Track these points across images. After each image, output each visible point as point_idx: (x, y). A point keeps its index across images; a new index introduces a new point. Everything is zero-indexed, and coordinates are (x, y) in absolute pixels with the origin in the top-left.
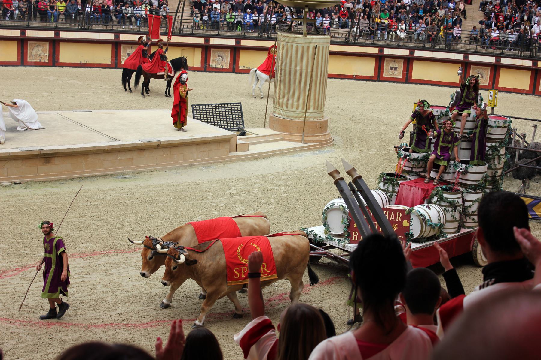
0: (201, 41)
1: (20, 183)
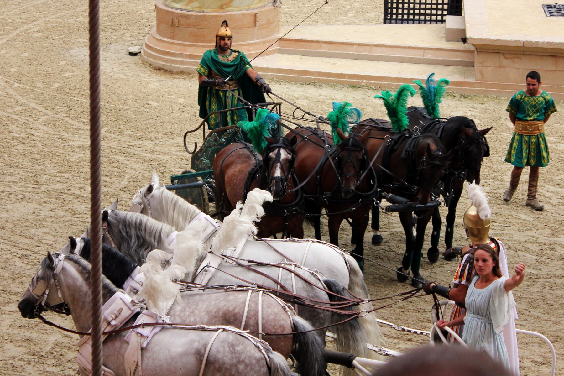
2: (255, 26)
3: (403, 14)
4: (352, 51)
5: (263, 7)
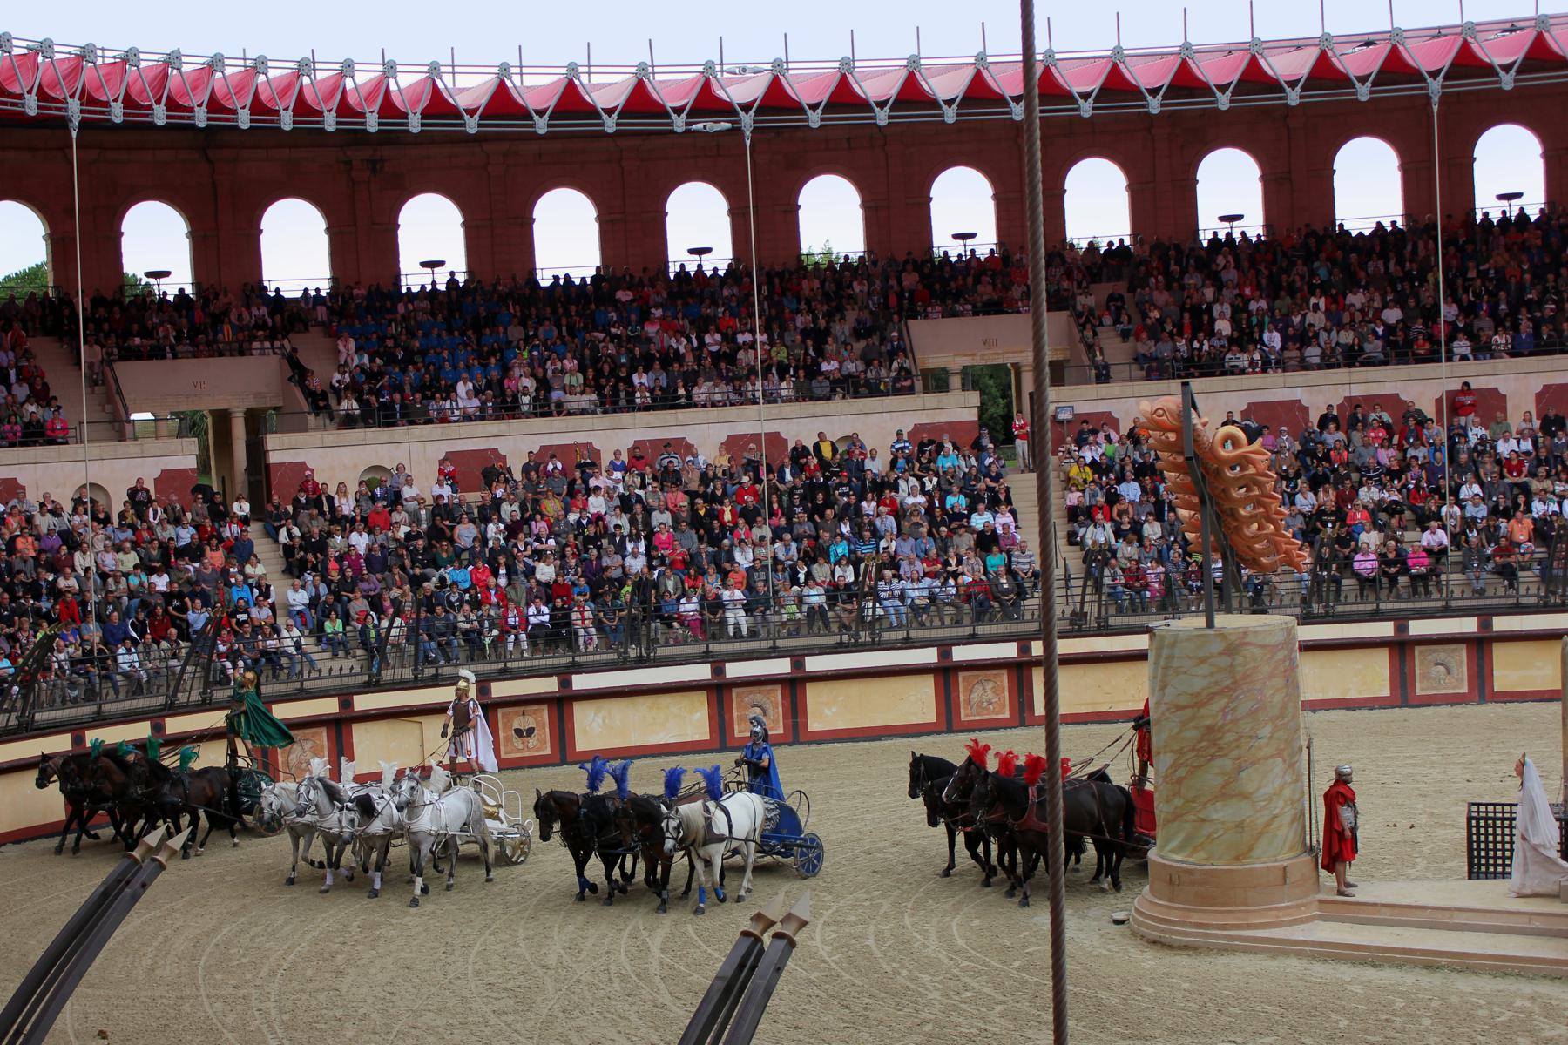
2: (1285, 883)
3: (1495, 865)
4: (1423, 917)
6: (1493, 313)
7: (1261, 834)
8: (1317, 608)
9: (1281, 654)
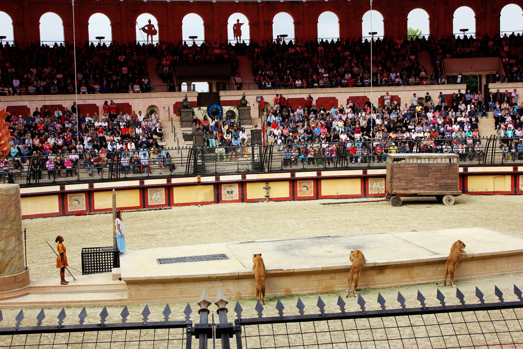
0: (510, 169)
1: (360, 290)
5: (20, 272)
6: (94, 78)
7: (7, 265)
8: (33, 181)
9: (14, 198)
